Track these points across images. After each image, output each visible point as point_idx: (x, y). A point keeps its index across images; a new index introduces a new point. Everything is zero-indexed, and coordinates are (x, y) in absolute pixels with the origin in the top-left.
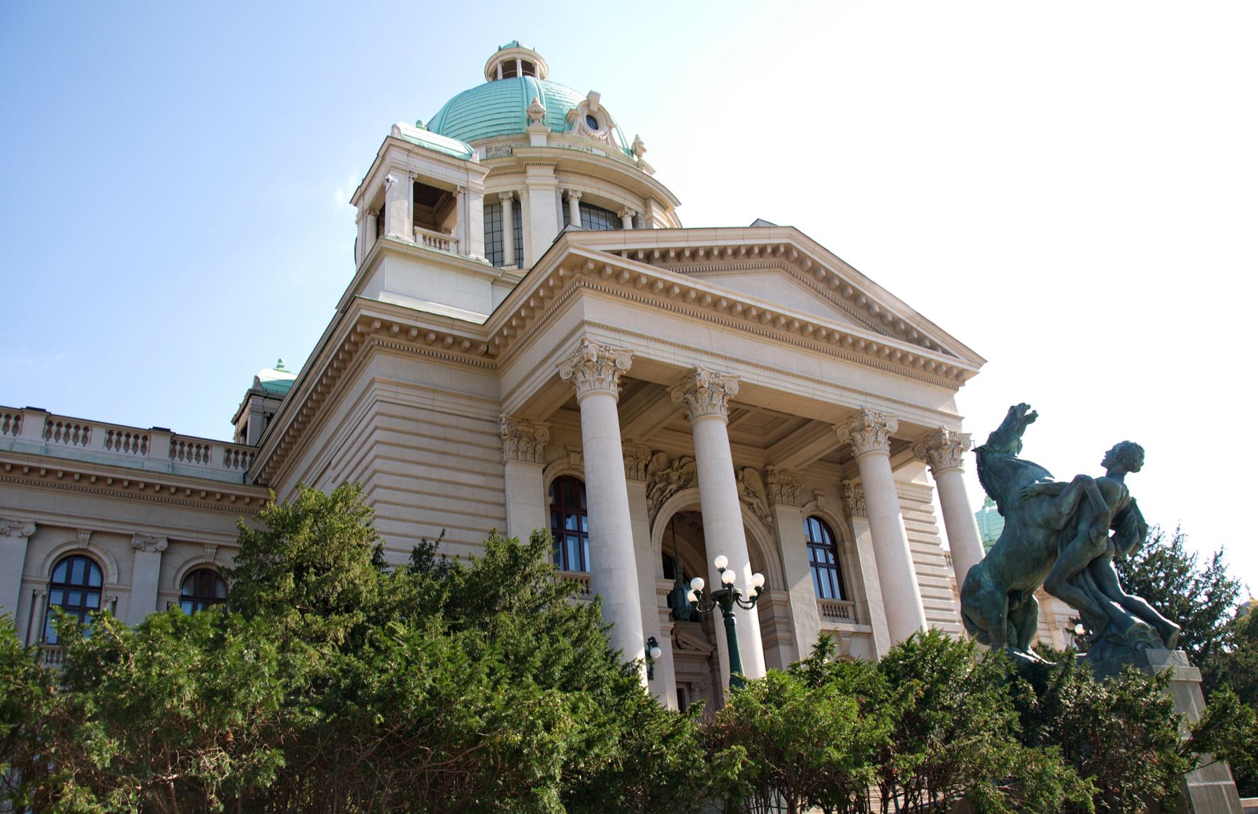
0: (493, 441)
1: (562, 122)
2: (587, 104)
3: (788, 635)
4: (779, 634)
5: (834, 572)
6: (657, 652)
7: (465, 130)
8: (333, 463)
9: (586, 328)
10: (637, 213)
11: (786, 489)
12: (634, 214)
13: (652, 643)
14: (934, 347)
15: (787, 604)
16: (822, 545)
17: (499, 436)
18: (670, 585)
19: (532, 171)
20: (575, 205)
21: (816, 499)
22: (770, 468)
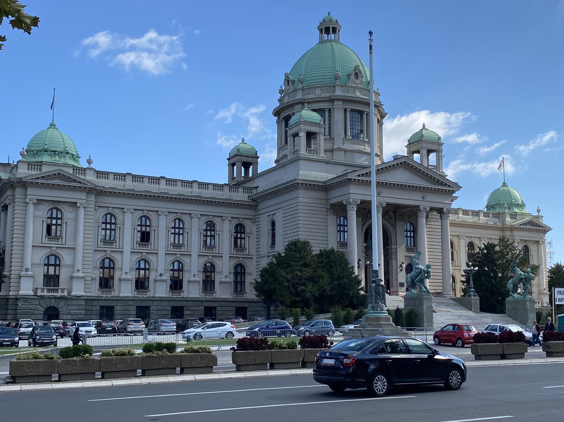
0: (325, 210)
1: (346, 77)
2: (355, 69)
3: (396, 257)
4: (393, 257)
5: (412, 239)
6: (360, 262)
7: (313, 78)
8: (284, 208)
9: (351, 194)
10: (368, 112)
11: (401, 217)
12: (367, 113)
13: (359, 260)
14: (445, 185)
15: (396, 249)
16: (410, 231)
17: (327, 208)
18: (365, 245)
19: (336, 103)
20: (348, 113)
21: (409, 218)
22: (396, 211)
